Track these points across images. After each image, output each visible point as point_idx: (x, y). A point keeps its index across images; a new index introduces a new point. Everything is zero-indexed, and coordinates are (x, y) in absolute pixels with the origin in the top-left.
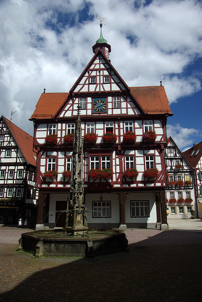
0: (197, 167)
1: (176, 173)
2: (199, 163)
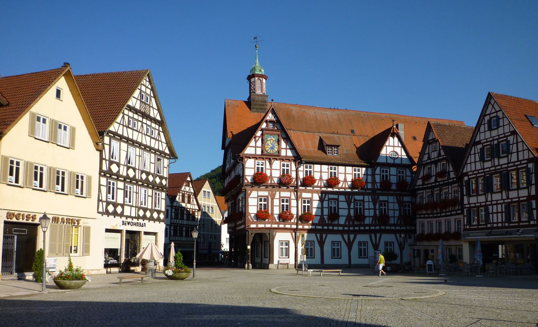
0: (465, 171)
1: (442, 187)
2: (468, 163)
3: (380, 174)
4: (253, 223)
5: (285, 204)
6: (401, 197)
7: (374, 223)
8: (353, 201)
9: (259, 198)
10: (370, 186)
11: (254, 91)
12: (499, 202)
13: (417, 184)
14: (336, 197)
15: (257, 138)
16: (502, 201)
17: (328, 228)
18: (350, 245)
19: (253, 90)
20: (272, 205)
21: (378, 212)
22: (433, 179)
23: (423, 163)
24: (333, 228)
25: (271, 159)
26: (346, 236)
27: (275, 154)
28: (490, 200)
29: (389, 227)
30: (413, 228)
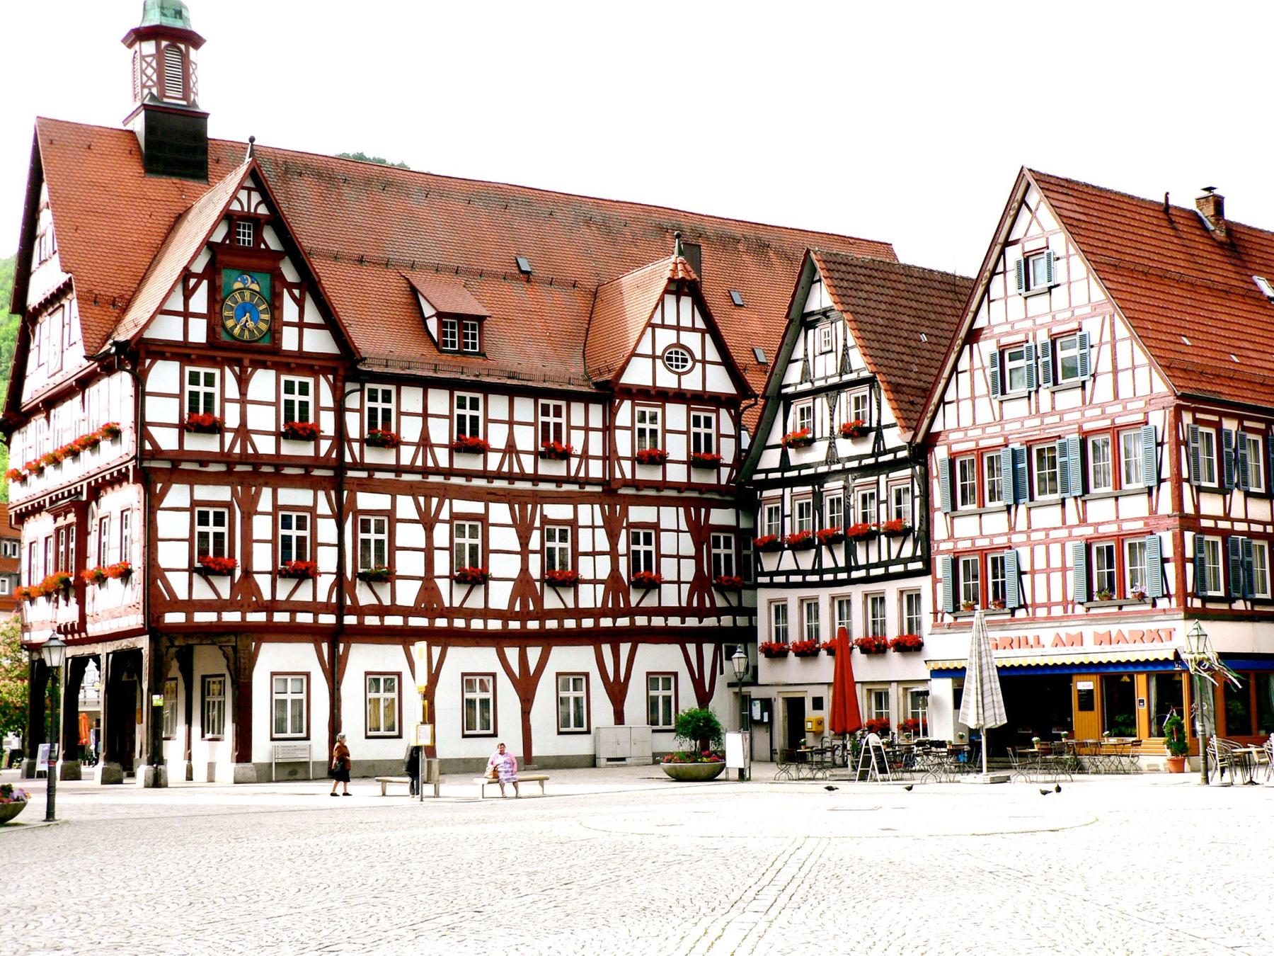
2: (947, 399)
3: (631, 428)
4: (176, 605)
5: (294, 533)
6: (703, 510)
7: (610, 606)
8: (537, 523)
9: (197, 509)
10: (596, 470)
11: (154, 91)
12: (1053, 534)
13: (761, 466)
14: (477, 507)
15: (192, 282)
16: (1063, 533)
17: (450, 623)
18: (526, 687)
19: (150, 88)
20: (248, 540)
21: (623, 562)
22: (818, 453)
23: (784, 391)
24: (468, 625)
25: (246, 362)
26: (512, 654)
27: (261, 344)
28: (1025, 528)
29: (662, 619)
30: (742, 621)
